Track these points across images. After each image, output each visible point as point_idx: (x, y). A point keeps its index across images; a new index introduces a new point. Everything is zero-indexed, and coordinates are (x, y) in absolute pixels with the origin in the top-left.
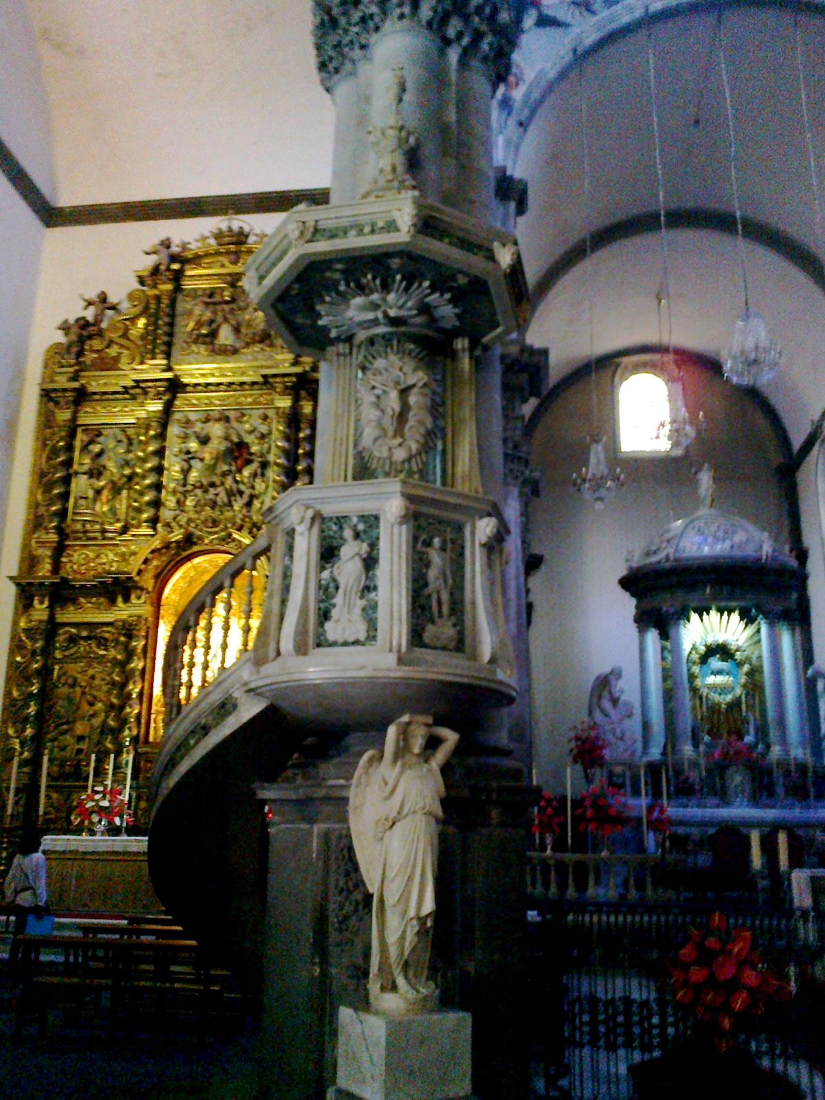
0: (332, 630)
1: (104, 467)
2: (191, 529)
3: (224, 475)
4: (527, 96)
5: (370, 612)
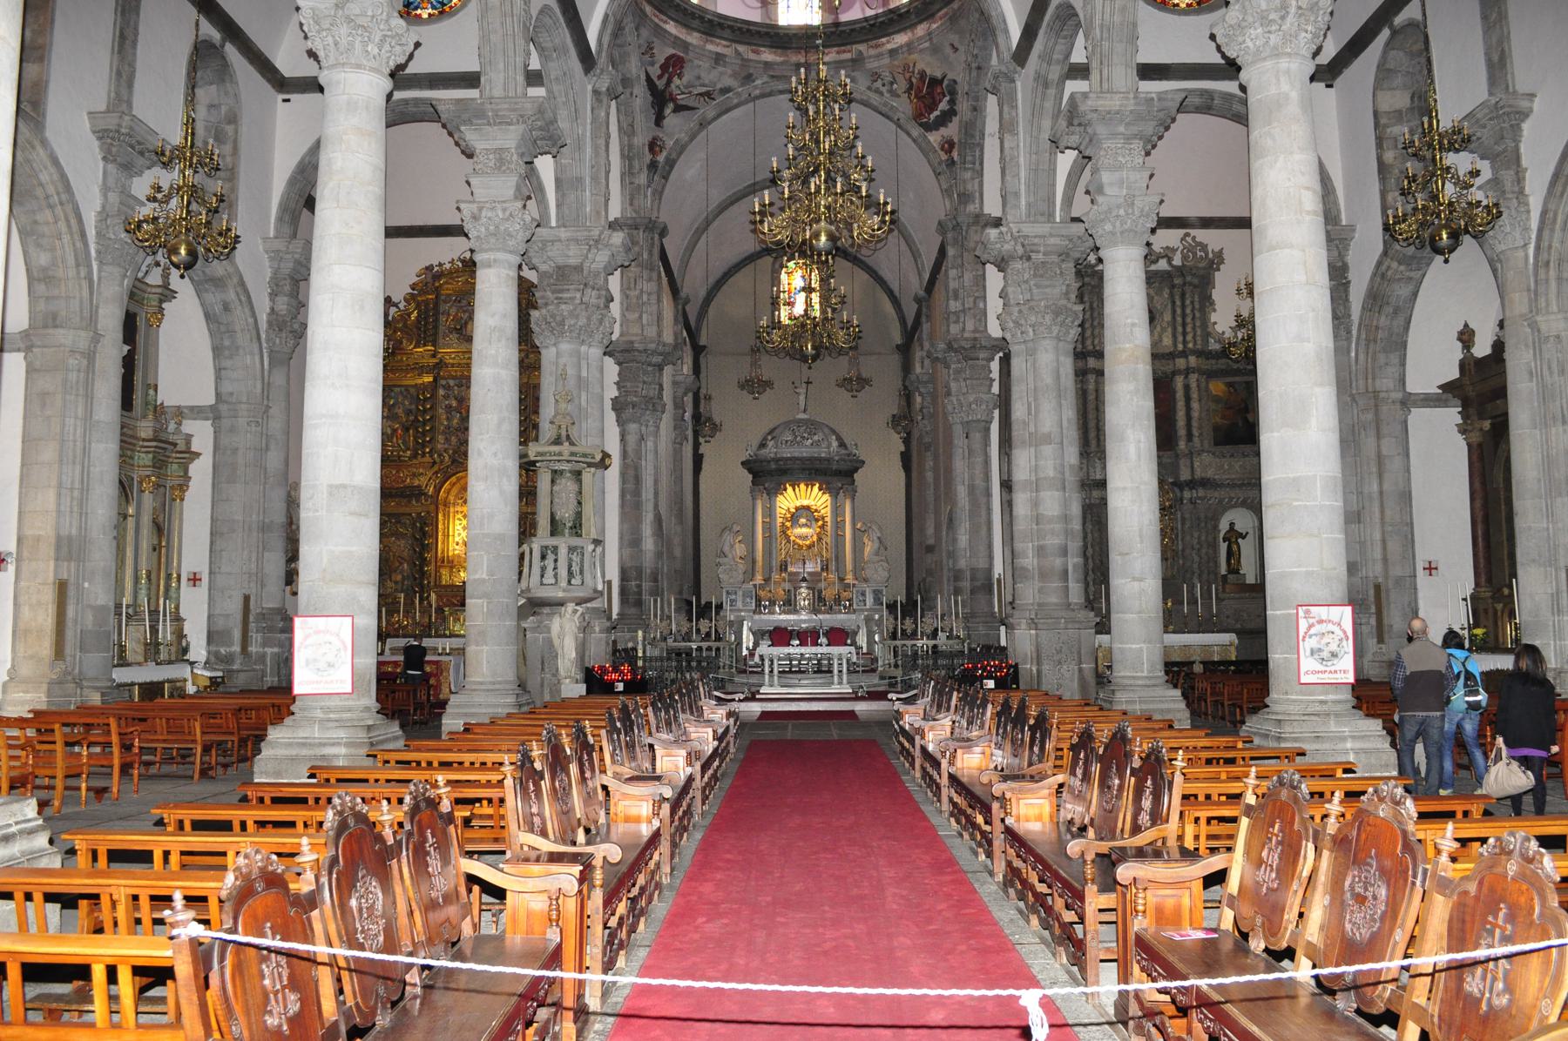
0: (545, 581)
4: (667, 159)
5: (556, 576)
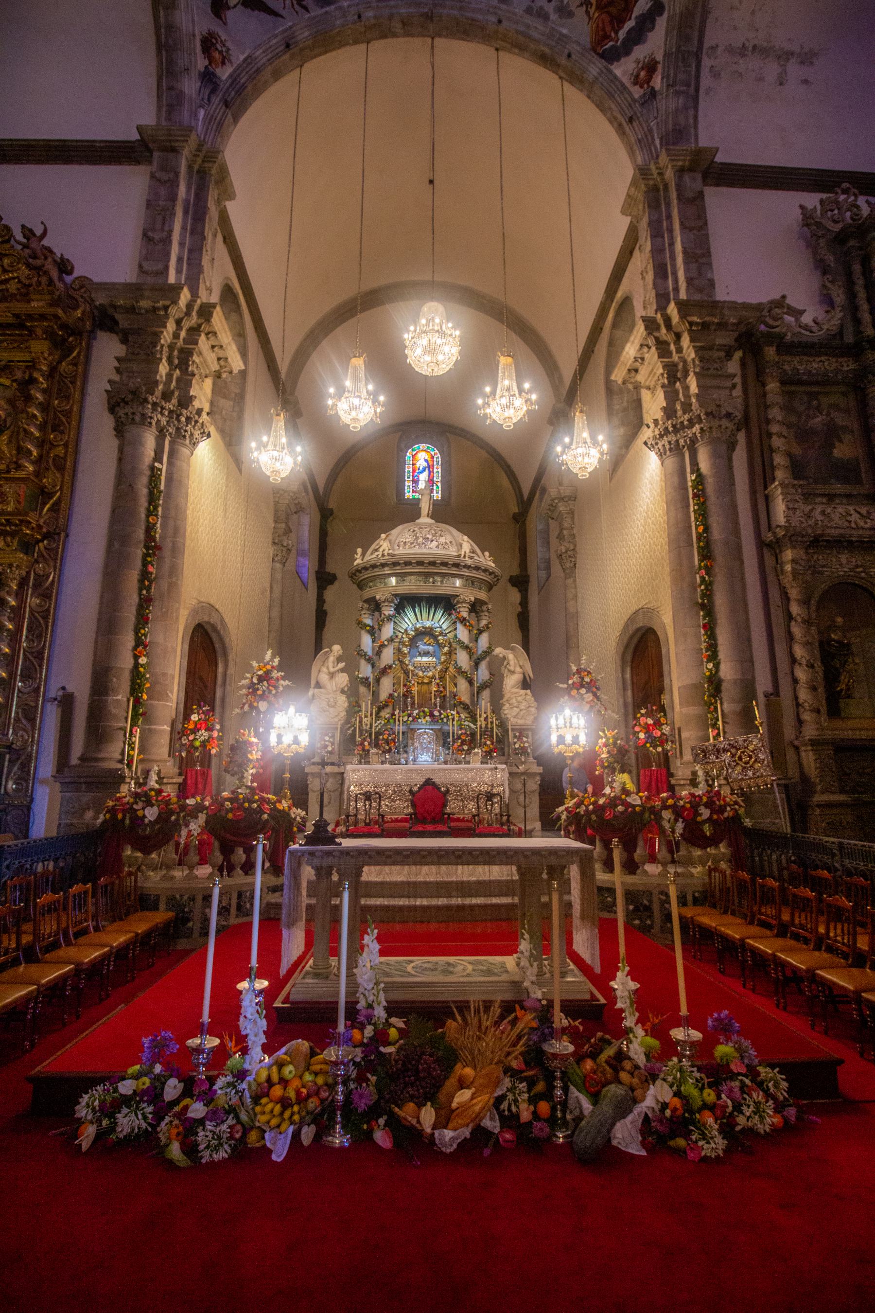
4: (234, 78)
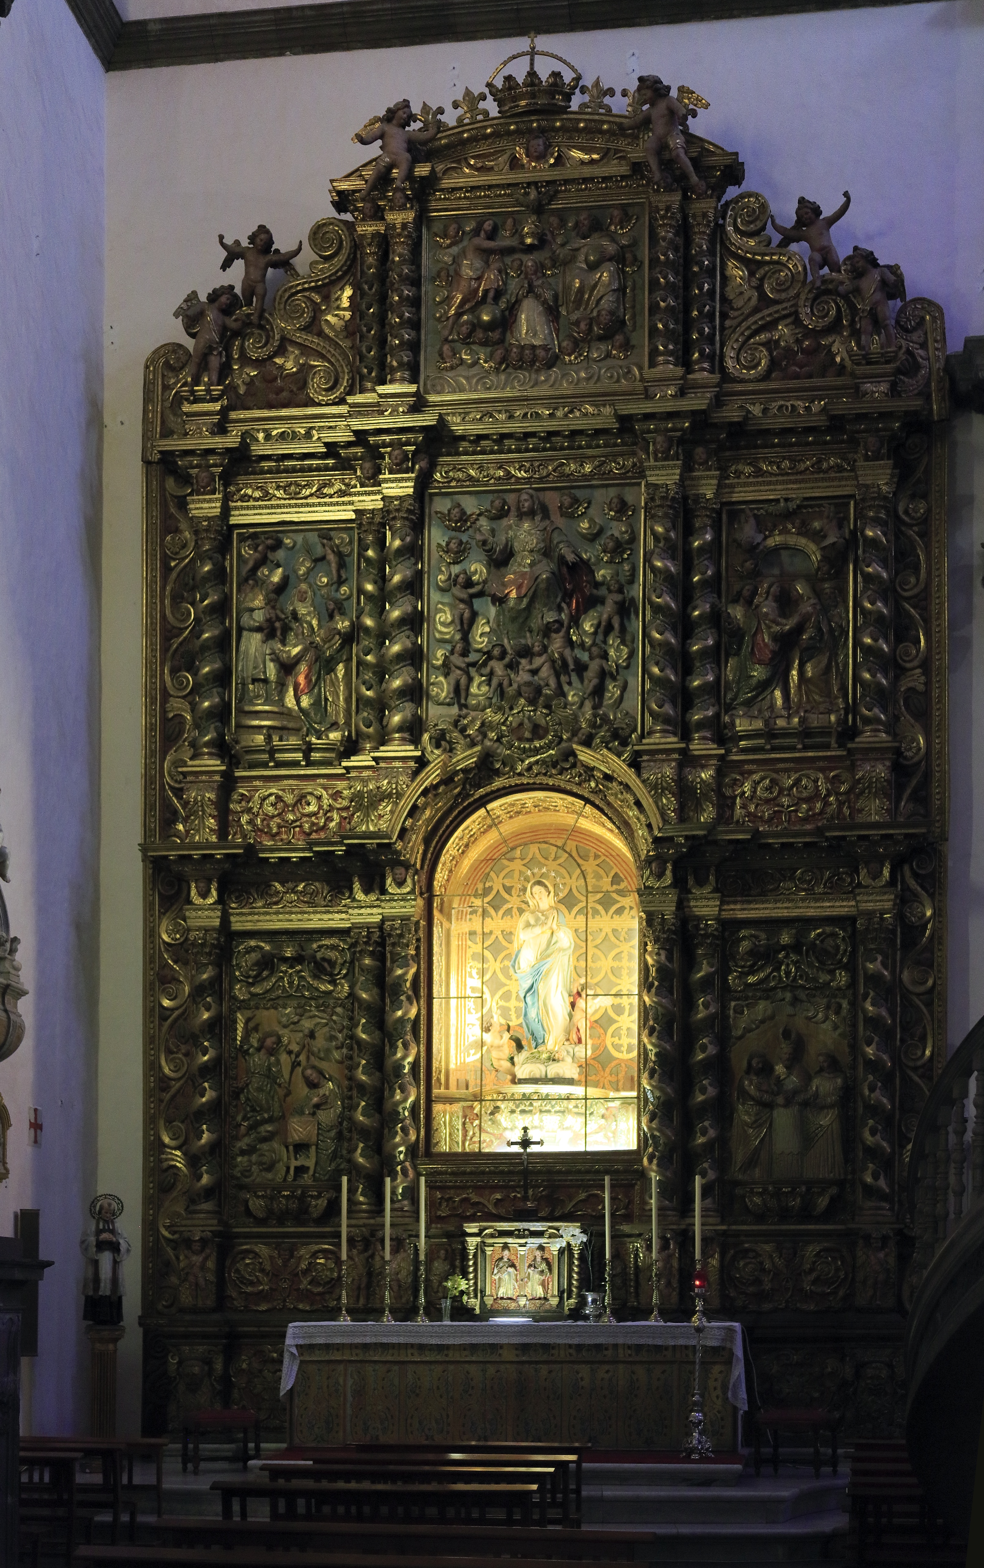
1: (295, 615)
2: (488, 743)
3: (547, 631)
